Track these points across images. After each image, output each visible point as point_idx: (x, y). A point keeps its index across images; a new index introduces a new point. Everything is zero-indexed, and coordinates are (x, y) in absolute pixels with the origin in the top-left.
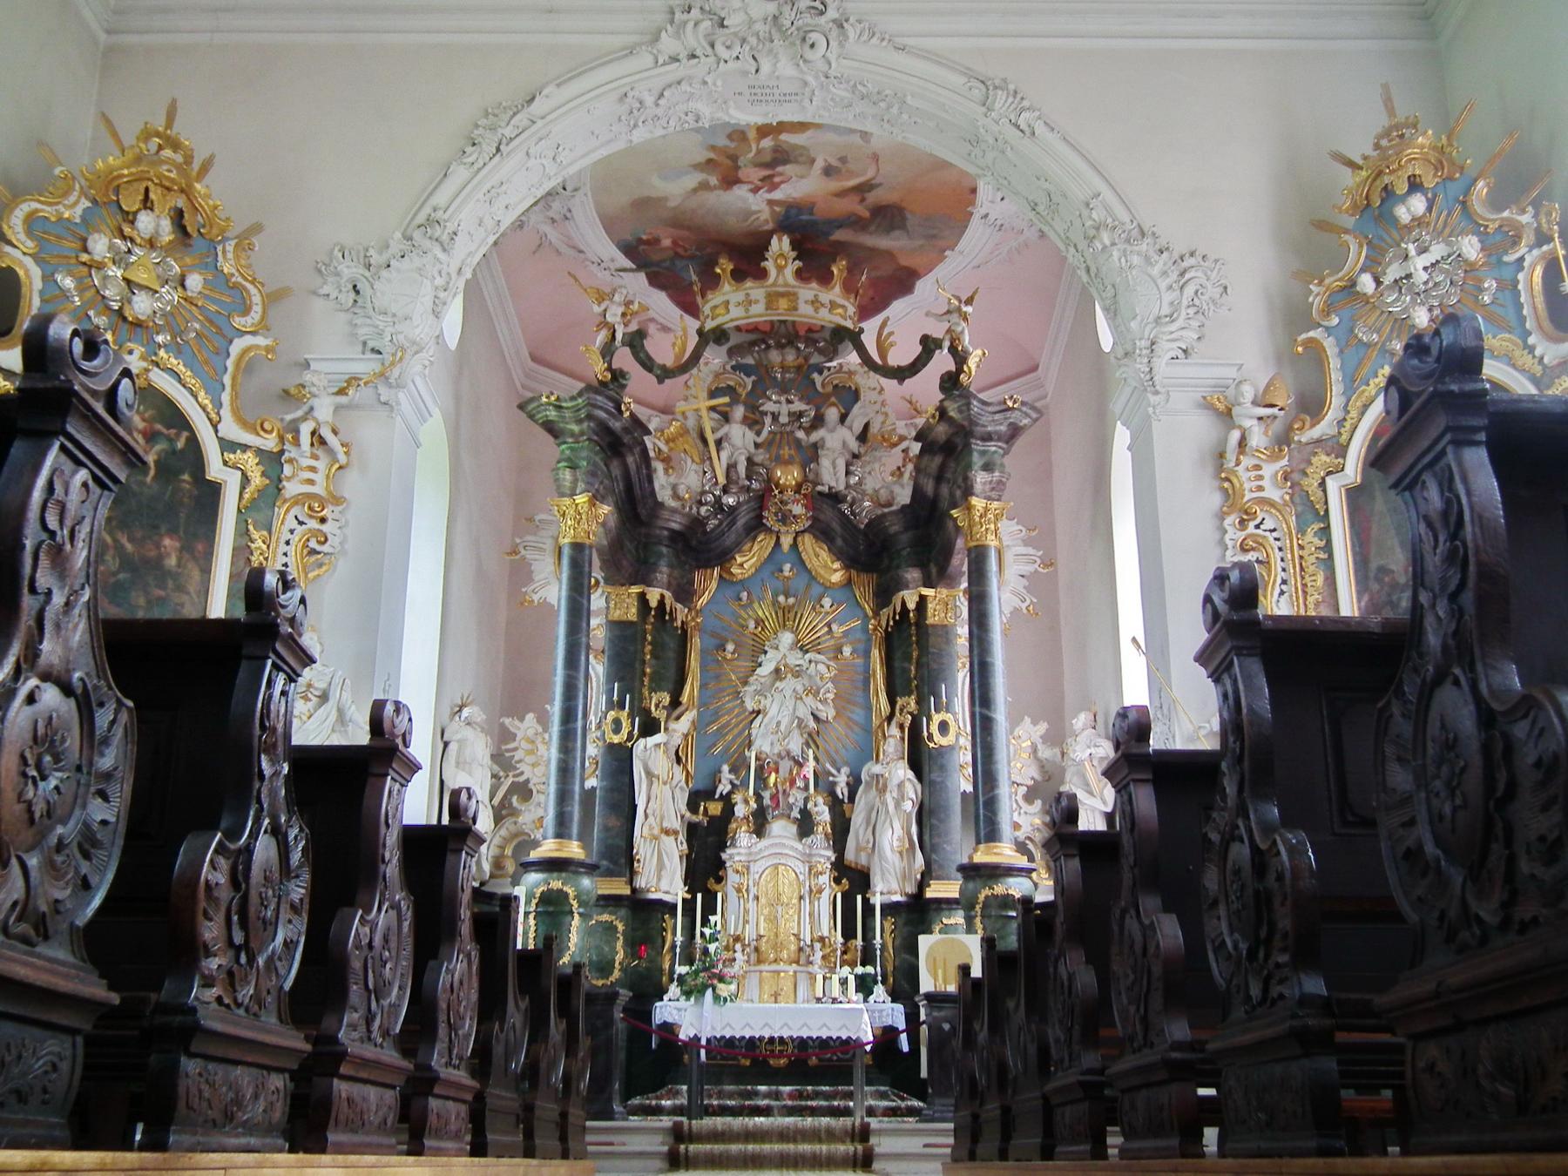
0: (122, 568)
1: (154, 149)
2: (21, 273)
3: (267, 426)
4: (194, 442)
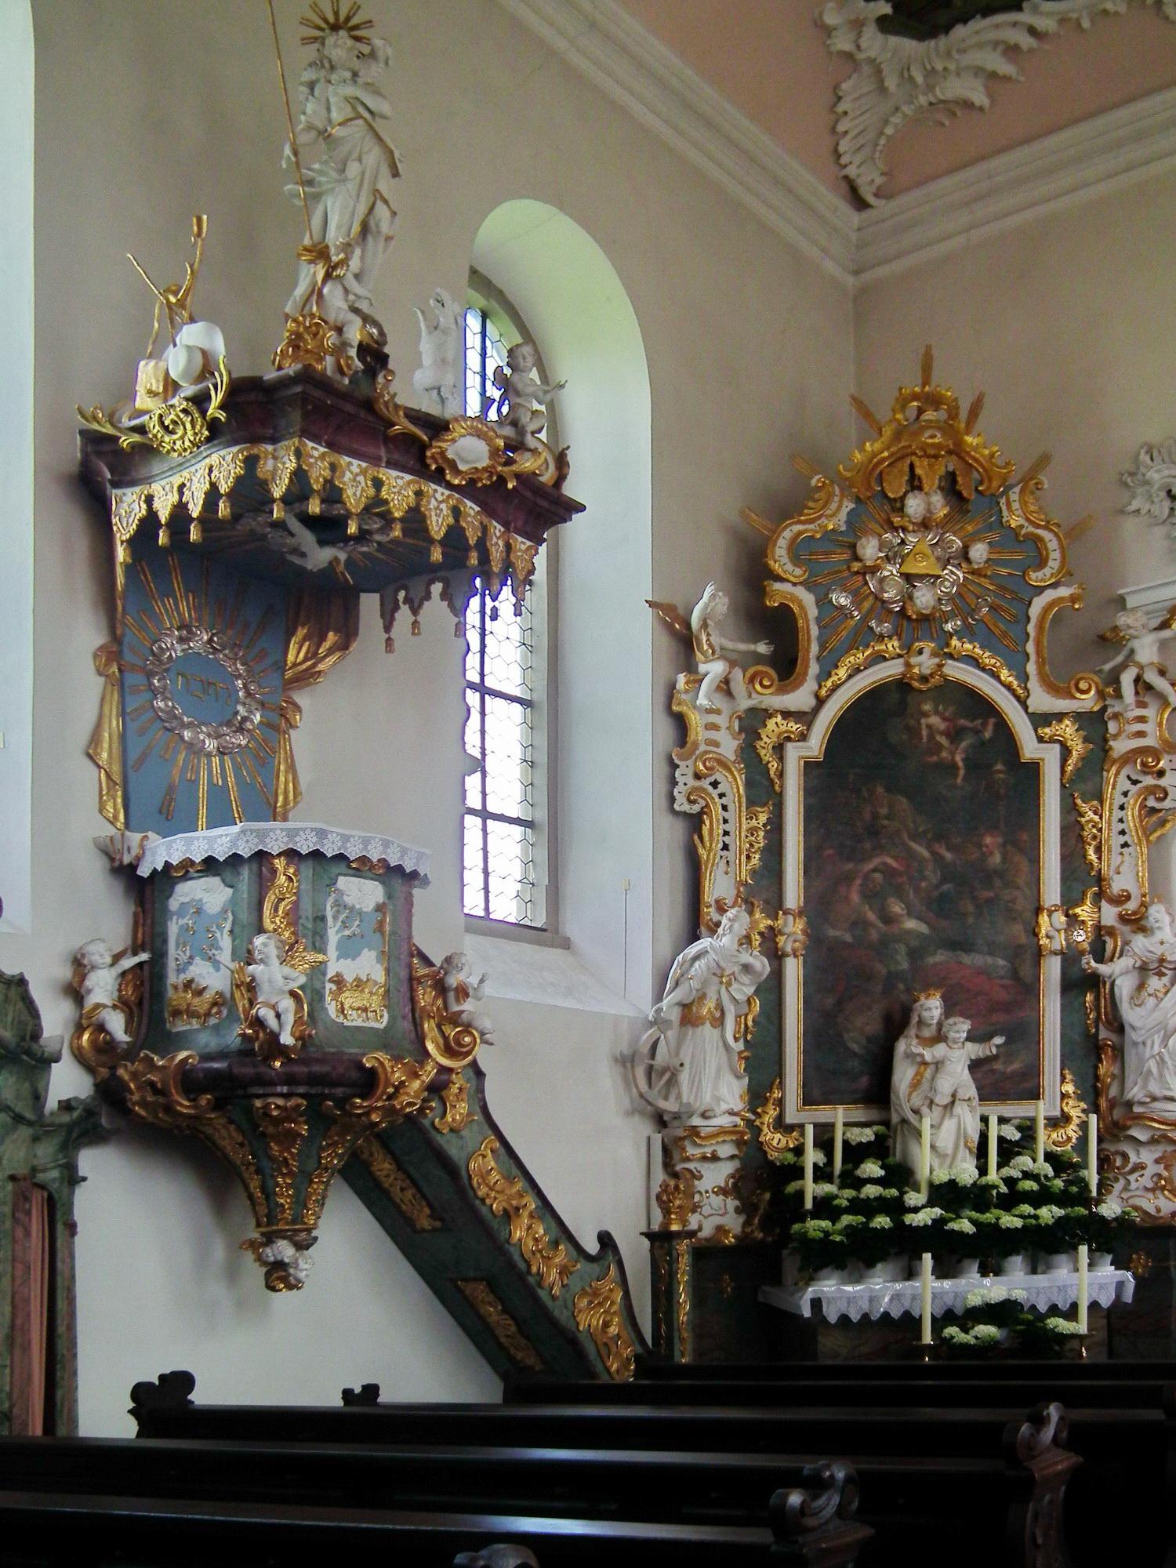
0: (944, 880)
1: (913, 414)
2: (796, 610)
3: (1083, 685)
4: (1004, 729)
